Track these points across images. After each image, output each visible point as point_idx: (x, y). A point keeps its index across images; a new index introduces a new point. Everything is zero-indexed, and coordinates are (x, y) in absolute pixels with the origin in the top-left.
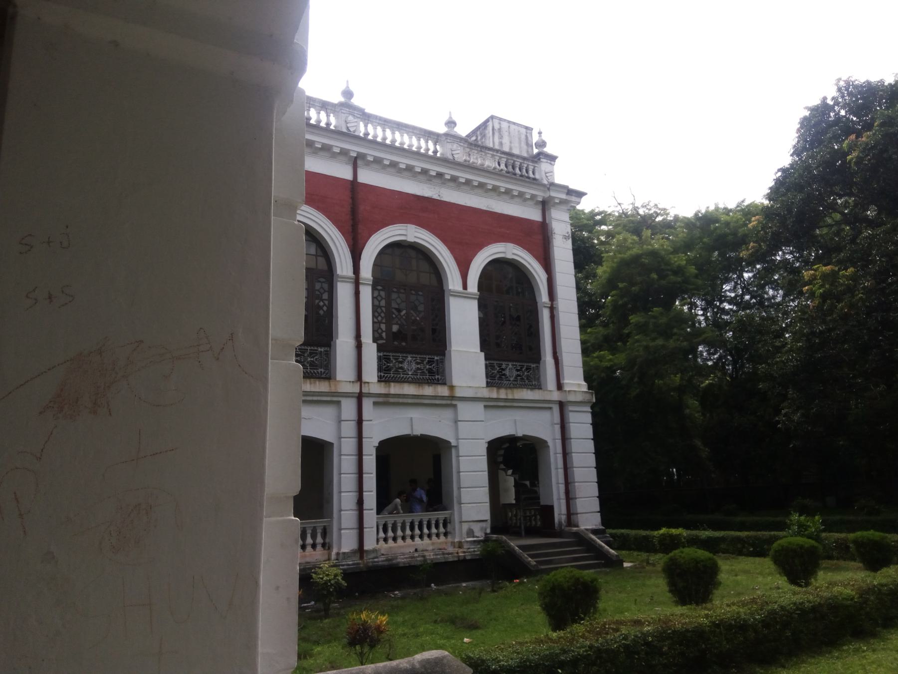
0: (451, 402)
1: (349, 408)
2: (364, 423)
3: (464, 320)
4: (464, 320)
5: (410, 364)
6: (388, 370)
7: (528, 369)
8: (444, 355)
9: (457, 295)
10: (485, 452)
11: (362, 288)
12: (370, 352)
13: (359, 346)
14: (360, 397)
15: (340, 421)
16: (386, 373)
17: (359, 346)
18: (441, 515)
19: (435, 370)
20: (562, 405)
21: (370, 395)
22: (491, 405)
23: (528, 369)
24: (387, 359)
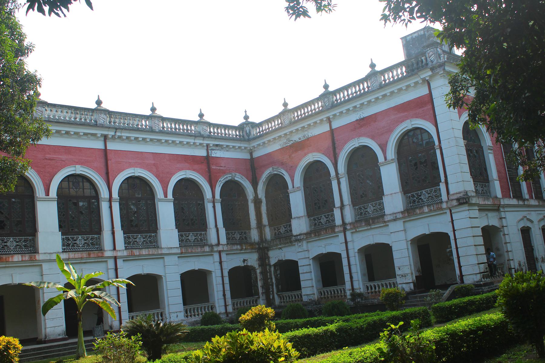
0: (161, 257)
1: (111, 263)
2: (118, 270)
3: (166, 212)
4: (166, 212)
5: (140, 238)
6: (129, 243)
7: (201, 235)
8: (157, 233)
9: (161, 200)
10: (179, 279)
11: (113, 204)
12: (120, 235)
13: (113, 233)
14: (115, 258)
15: (108, 269)
16: (128, 244)
17: (113, 233)
18: (159, 311)
19: (153, 242)
20: (220, 252)
21: (121, 257)
22: (181, 256)
23: (201, 235)
24: (129, 238)
